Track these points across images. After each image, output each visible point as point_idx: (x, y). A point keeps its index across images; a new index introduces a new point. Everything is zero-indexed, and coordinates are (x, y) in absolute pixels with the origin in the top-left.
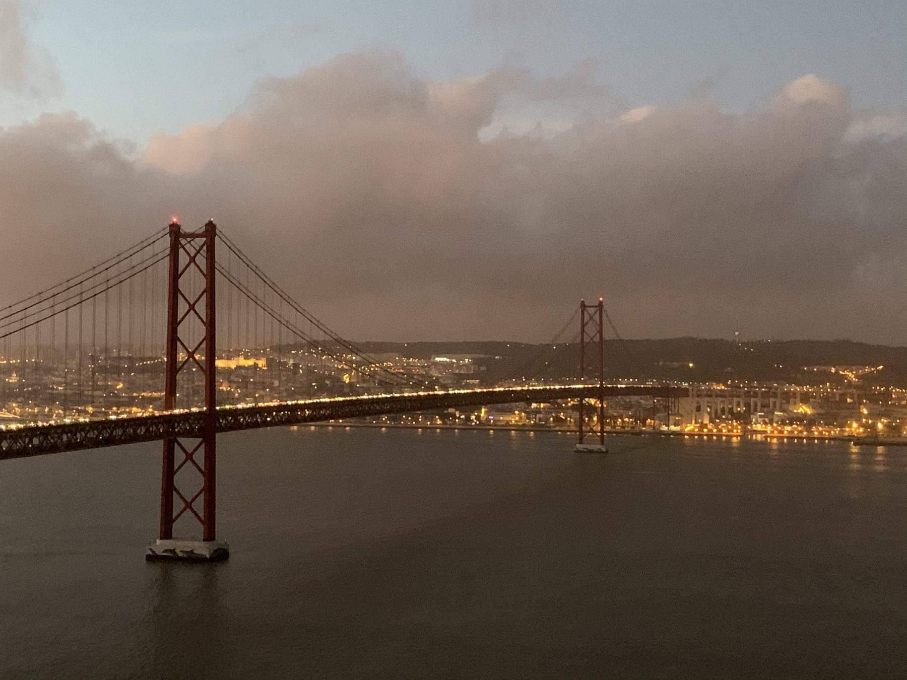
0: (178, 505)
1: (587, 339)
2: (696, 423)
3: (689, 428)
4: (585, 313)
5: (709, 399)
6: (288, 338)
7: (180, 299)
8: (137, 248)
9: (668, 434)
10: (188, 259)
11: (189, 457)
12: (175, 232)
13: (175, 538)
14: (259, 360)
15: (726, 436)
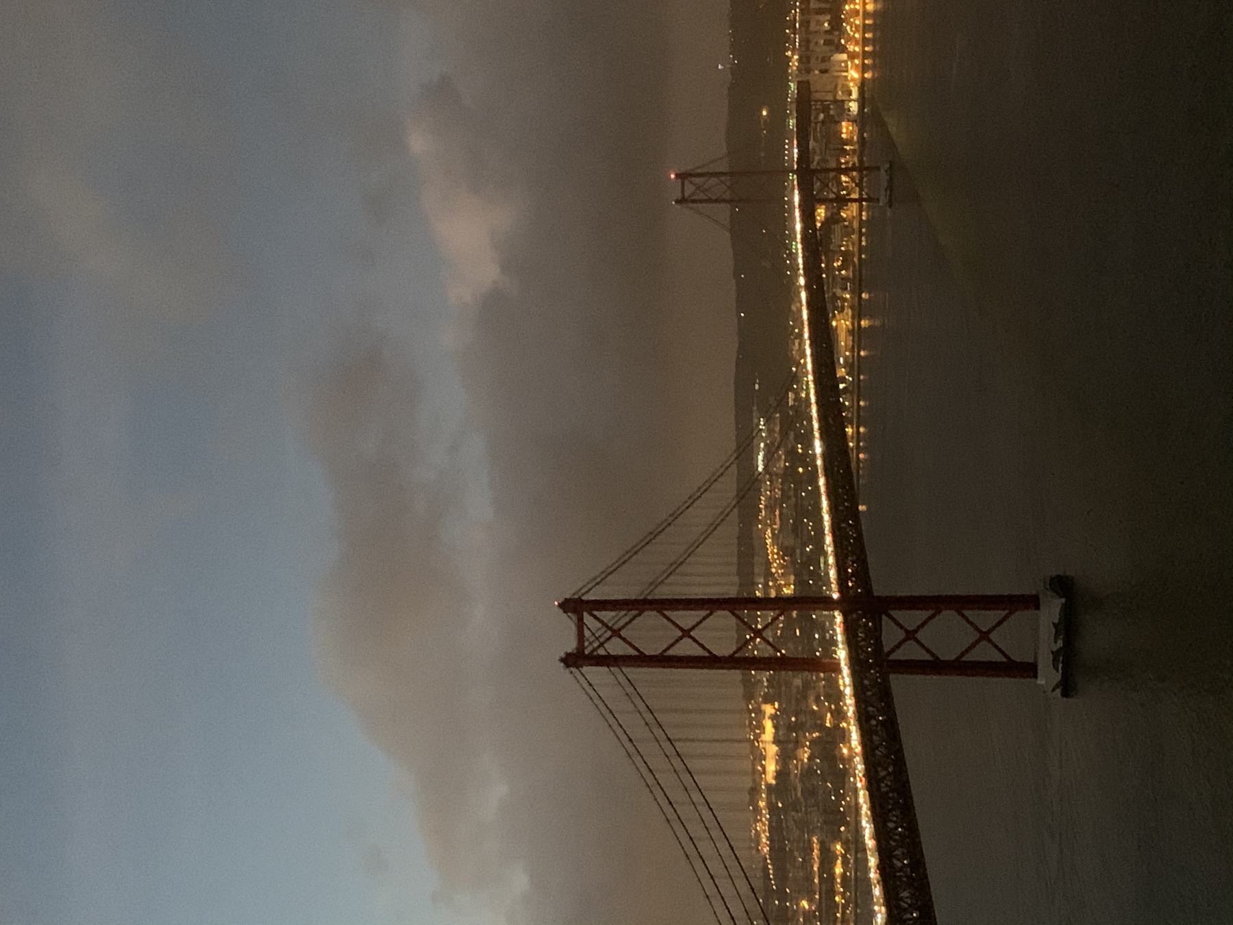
0: (984, 653)
1: (727, 196)
2: (847, 71)
3: (854, 74)
4: (693, 198)
5: (812, 61)
6: (731, 528)
7: (671, 652)
8: (601, 706)
9: (862, 101)
10: (616, 640)
11: (910, 635)
12: (573, 660)
13: (1036, 658)
14: (765, 713)
15: (864, 19)
